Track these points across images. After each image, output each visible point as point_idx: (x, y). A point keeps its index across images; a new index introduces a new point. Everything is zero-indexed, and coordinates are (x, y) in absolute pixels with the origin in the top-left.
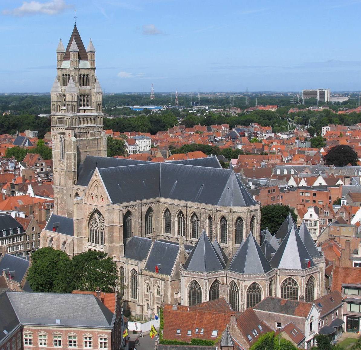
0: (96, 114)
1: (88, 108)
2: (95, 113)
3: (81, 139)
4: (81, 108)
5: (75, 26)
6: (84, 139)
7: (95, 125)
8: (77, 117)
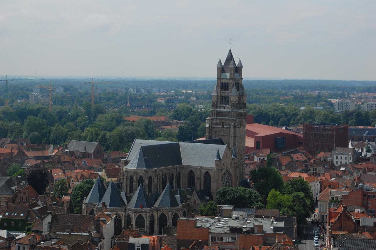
0: (230, 110)
1: (227, 106)
3: (218, 126)
4: (222, 105)
5: (230, 49)
6: (219, 126)
7: (228, 118)
8: (216, 112)
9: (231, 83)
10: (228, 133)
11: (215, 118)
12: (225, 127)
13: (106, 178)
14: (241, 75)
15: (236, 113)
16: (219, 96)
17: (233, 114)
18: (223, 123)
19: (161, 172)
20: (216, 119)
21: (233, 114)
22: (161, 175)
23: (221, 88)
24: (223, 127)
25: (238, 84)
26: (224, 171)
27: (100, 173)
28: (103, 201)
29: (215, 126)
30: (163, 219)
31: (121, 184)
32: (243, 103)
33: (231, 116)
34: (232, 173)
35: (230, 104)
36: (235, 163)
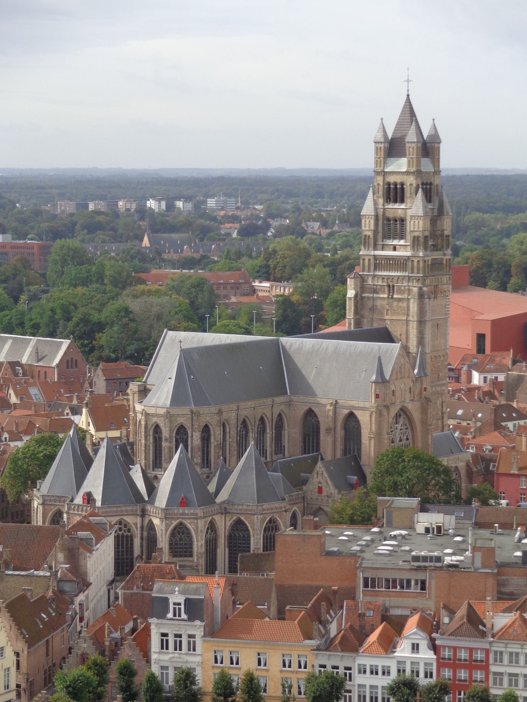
0: (409, 254)
1: (402, 242)
2: (408, 253)
5: (408, 96)
8: (372, 258)
9: (411, 185)
10: (403, 312)
11: (370, 275)
12: (395, 296)
13: (92, 429)
14: (436, 161)
15: (425, 261)
16: (381, 217)
17: (415, 263)
18: (391, 289)
19: (233, 415)
20: (374, 276)
21: (415, 263)
22: (233, 421)
23: (385, 196)
24: (392, 298)
25: (428, 186)
26: (394, 411)
27: (76, 419)
28: (86, 488)
29: (371, 295)
30: (239, 535)
31: (132, 445)
32: (442, 235)
33: (412, 269)
34: (416, 416)
35: (409, 237)
36: (423, 389)
